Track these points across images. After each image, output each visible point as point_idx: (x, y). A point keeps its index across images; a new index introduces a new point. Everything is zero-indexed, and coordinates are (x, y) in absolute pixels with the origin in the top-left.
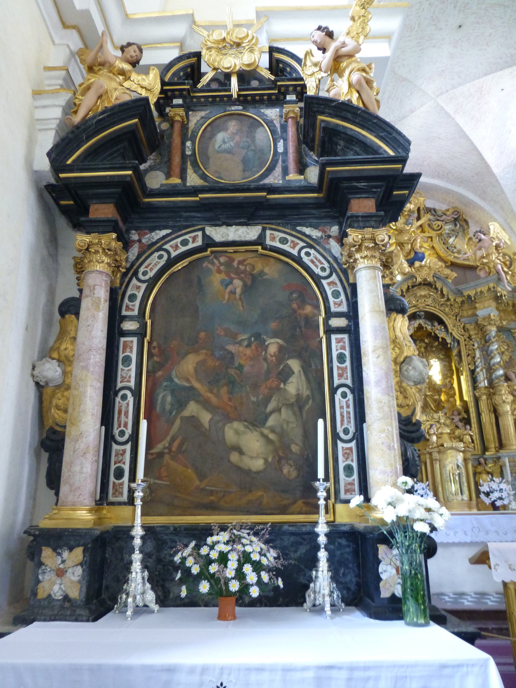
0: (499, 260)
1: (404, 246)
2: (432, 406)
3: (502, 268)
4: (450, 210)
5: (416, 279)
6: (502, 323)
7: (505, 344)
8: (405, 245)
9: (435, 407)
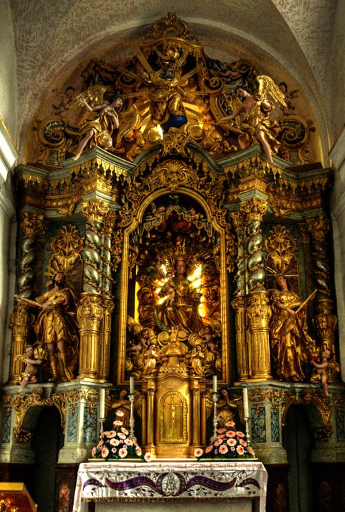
0: (264, 125)
1: (157, 107)
2: (184, 323)
3: (267, 136)
4: (237, 64)
5: (162, 151)
7: (288, 241)
8: (160, 105)
9: (187, 323)
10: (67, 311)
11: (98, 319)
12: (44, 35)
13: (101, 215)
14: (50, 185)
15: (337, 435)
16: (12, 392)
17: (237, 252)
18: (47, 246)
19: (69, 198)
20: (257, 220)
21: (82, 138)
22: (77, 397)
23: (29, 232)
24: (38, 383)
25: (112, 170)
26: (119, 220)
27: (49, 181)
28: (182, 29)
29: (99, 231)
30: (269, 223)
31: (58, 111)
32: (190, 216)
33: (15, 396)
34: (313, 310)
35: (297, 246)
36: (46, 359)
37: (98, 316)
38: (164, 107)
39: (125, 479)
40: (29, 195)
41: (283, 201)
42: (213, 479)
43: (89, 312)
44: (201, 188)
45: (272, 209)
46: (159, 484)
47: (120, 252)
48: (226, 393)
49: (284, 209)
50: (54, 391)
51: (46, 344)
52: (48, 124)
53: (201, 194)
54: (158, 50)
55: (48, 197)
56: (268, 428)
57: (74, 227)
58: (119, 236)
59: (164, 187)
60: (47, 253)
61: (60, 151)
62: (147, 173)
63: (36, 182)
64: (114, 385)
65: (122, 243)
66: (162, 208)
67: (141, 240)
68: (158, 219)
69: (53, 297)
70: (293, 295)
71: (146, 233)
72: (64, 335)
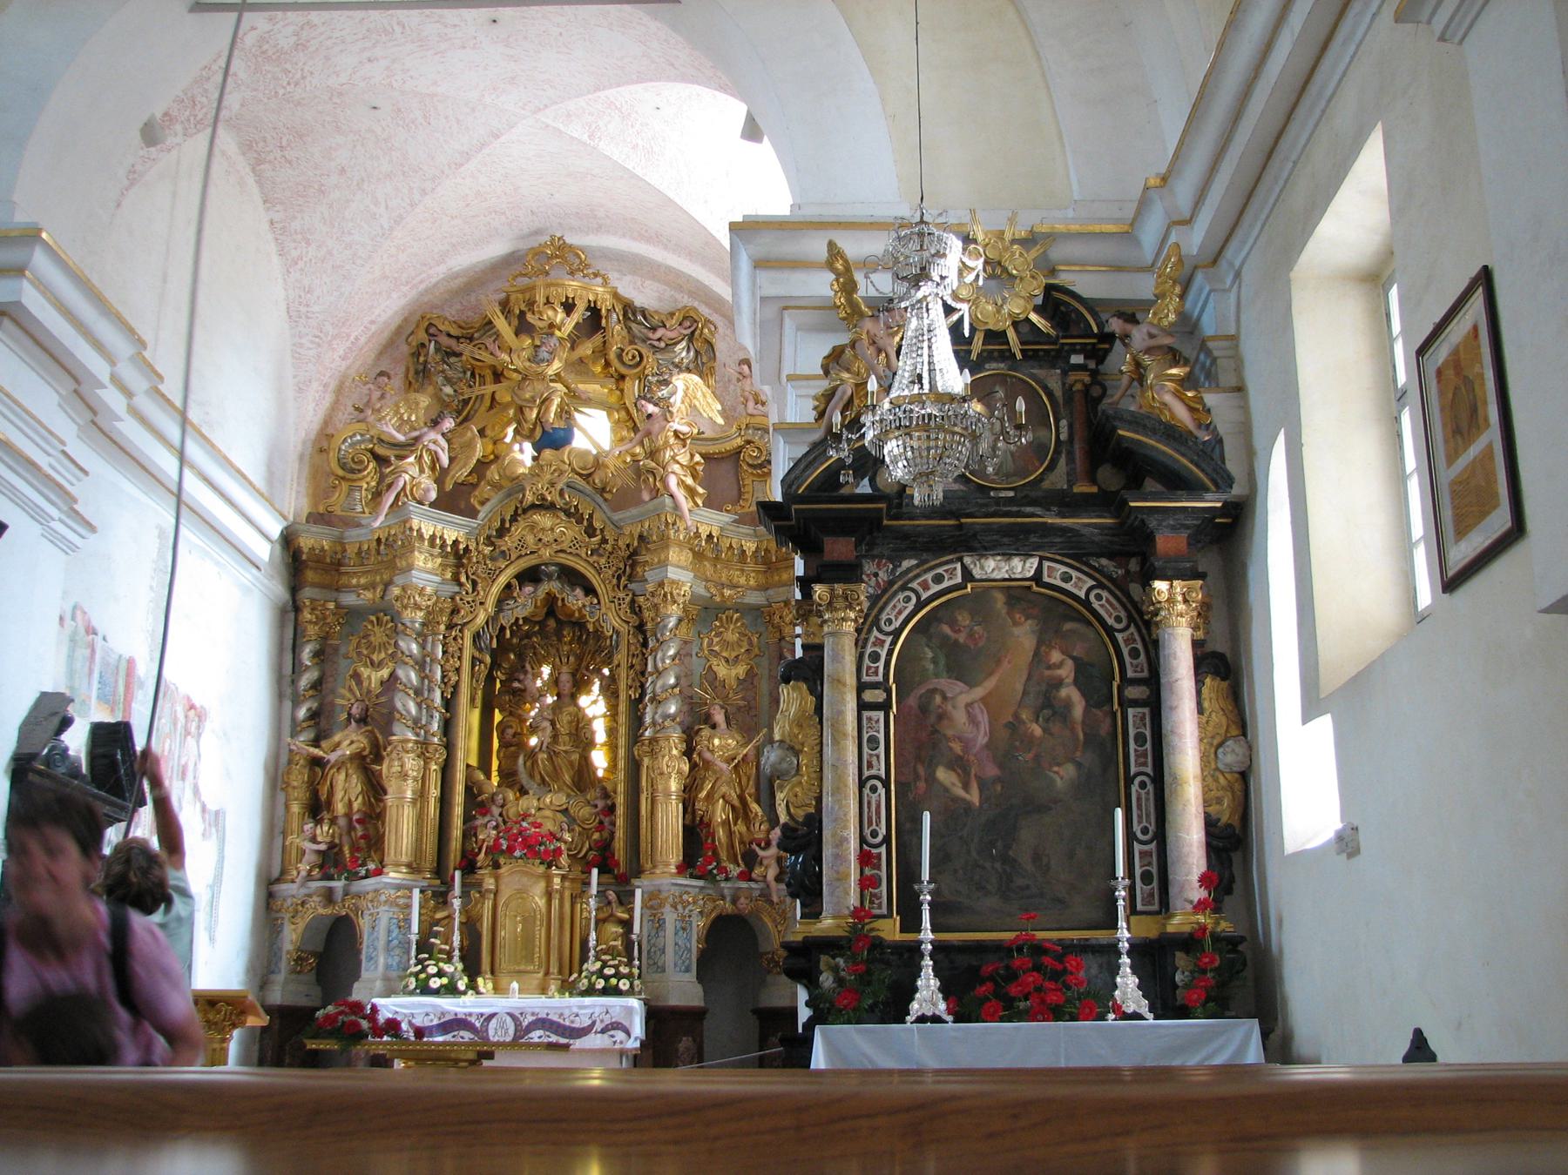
0: (678, 463)
3: (681, 483)
5: (524, 496)
6: (723, 595)
7: (745, 639)
8: (527, 411)
10: (368, 764)
12: (335, 293)
13: (421, 609)
14: (344, 551)
16: (285, 894)
17: (646, 665)
18: (343, 650)
19: (376, 572)
20: (673, 613)
21: (387, 490)
22: (378, 901)
23: (312, 630)
25: (438, 535)
26: (455, 611)
27: (343, 545)
28: (578, 261)
29: (419, 634)
30: (705, 613)
31: (362, 416)
33: (289, 901)
35: (759, 649)
36: (337, 841)
37: (415, 774)
38: (534, 416)
39: (436, 1022)
40: (311, 568)
42: (562, 1021)
43: (399, 769)
44: (592, 554)
46: (484, 1029)
47: (457, 665)
48: (614, 895)
49: (734, 586)
50: (346, 893)
51: (336, 817)
52: (345, 440)
53: (592, 565)
54: (529, 310)
55: (343, 569)
56: (670, 950)
57: (389, 617)
60: (343, 663)
61: (365, 486)
62: (502, 532)
63: (322, 549)
64: (442, 883)
65: (460, 649)
66: (529, 589)
67: (495, 640)
68: (526, 603)
69: (348, 742)
70: (733, 738)
72: (364, 803)
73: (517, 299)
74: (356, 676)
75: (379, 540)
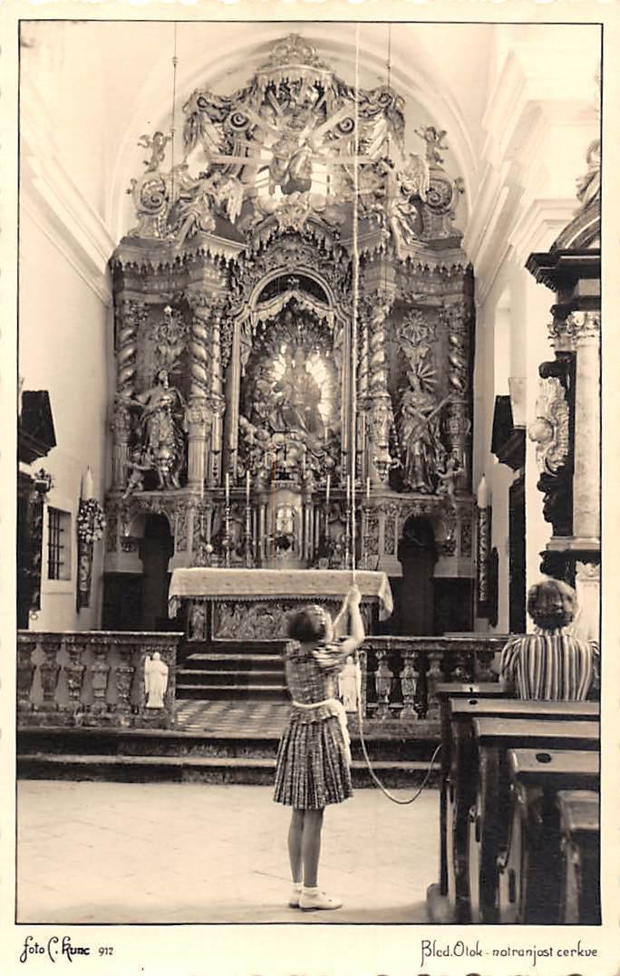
2: (303, 425)
4: (376, 94)
5: (278, 227)
6: (412, 298)
7: (425, 329)
11: (208, 425)
13: (208, 307)
15: (462, 550)
24: (145, 490)
25: (220, 255)
32: (308, 303)
34: (446, 414)
41: (419, 283)
45: (403, 295)
58: (229, 325)
59: (282, 267)
67: (255, 331)
68: (276, 306)
71: (260, 322)
73: (263, 79)
74: (158, 351)
75: (178, 258)
